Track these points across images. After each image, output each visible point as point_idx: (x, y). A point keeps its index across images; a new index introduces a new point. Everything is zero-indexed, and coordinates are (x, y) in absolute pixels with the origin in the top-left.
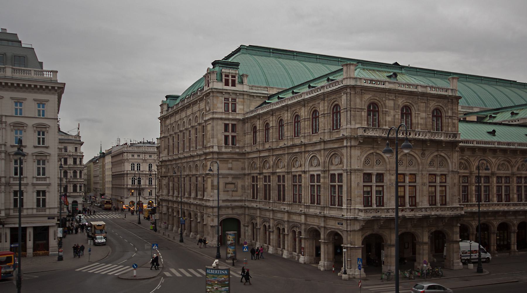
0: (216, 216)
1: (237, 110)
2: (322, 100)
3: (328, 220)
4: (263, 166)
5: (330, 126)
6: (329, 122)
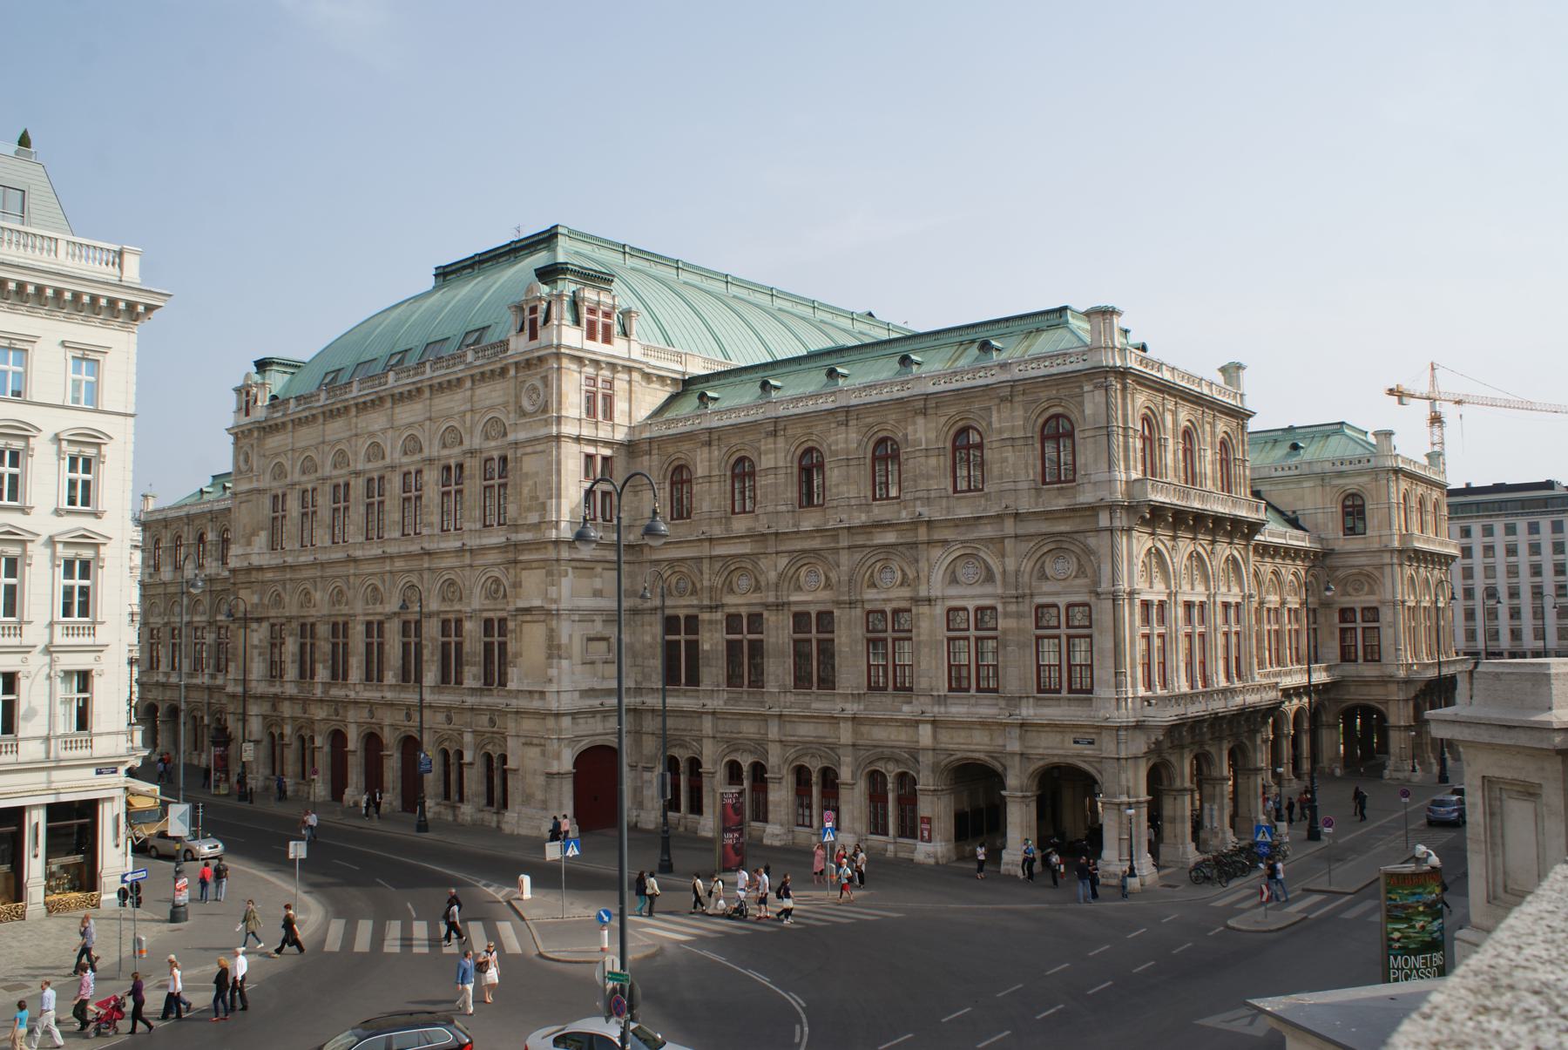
0: (566, 742)
1: (617, 414)
2: (1003, 400)
3: (1029, 734)
4: (723, 585)
5: (1033, 473)
6: (1030, 461)
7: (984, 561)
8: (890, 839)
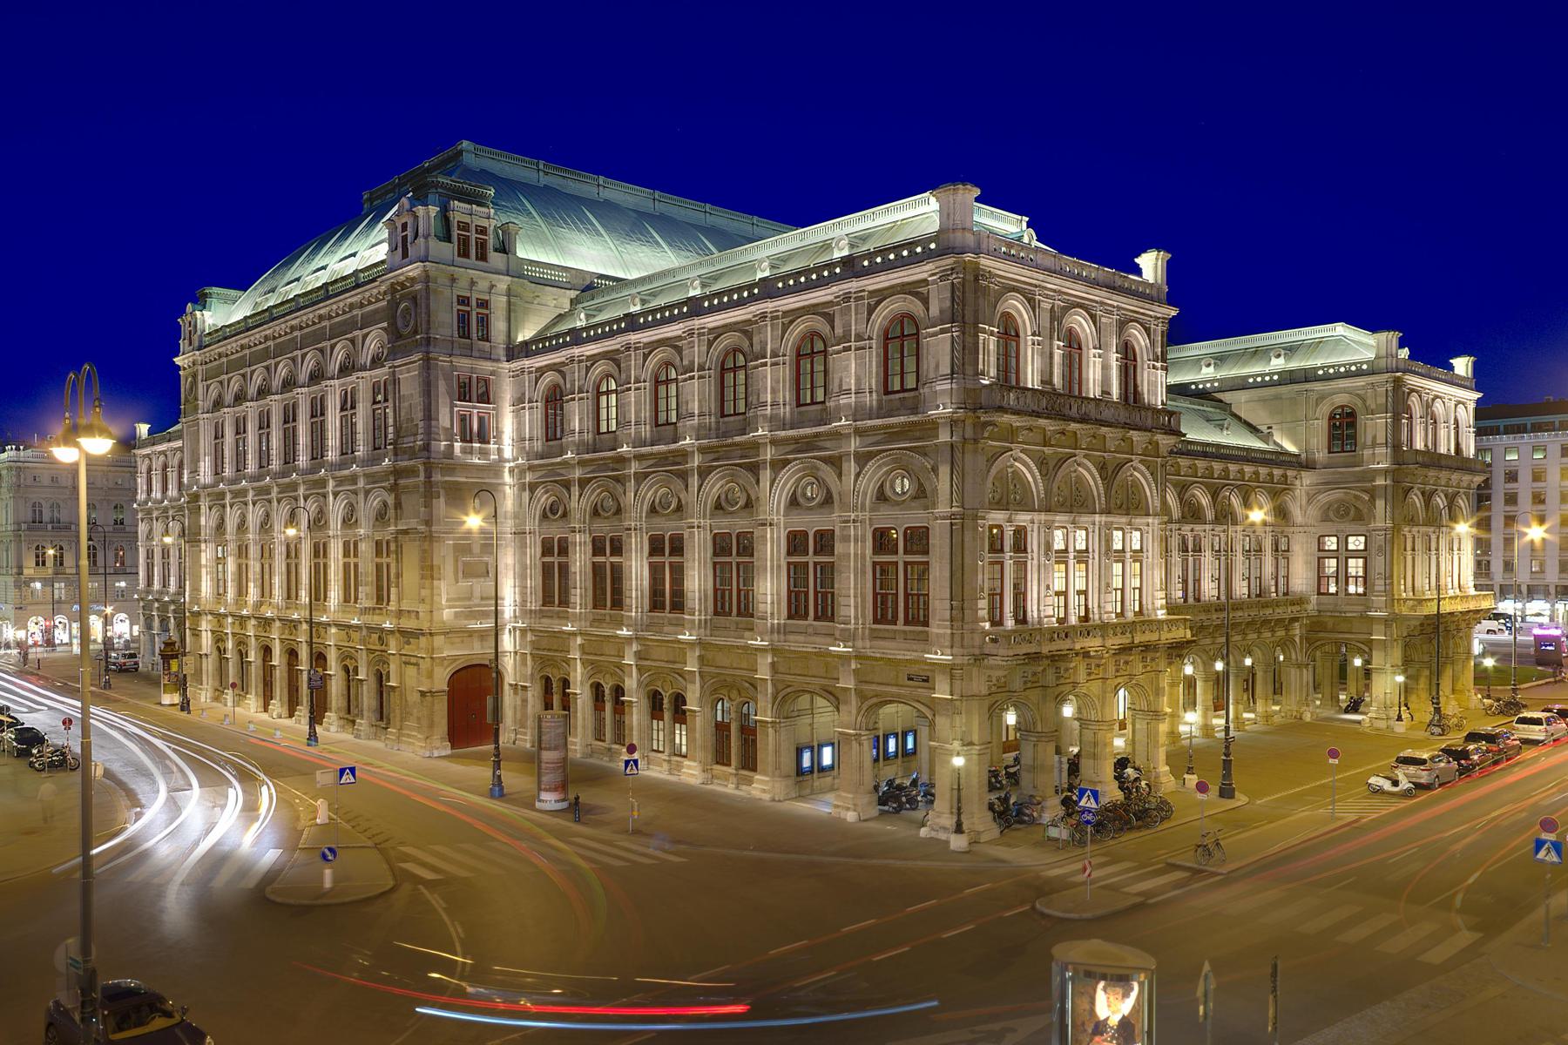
7: (824, 480)
8: (731, 770)
